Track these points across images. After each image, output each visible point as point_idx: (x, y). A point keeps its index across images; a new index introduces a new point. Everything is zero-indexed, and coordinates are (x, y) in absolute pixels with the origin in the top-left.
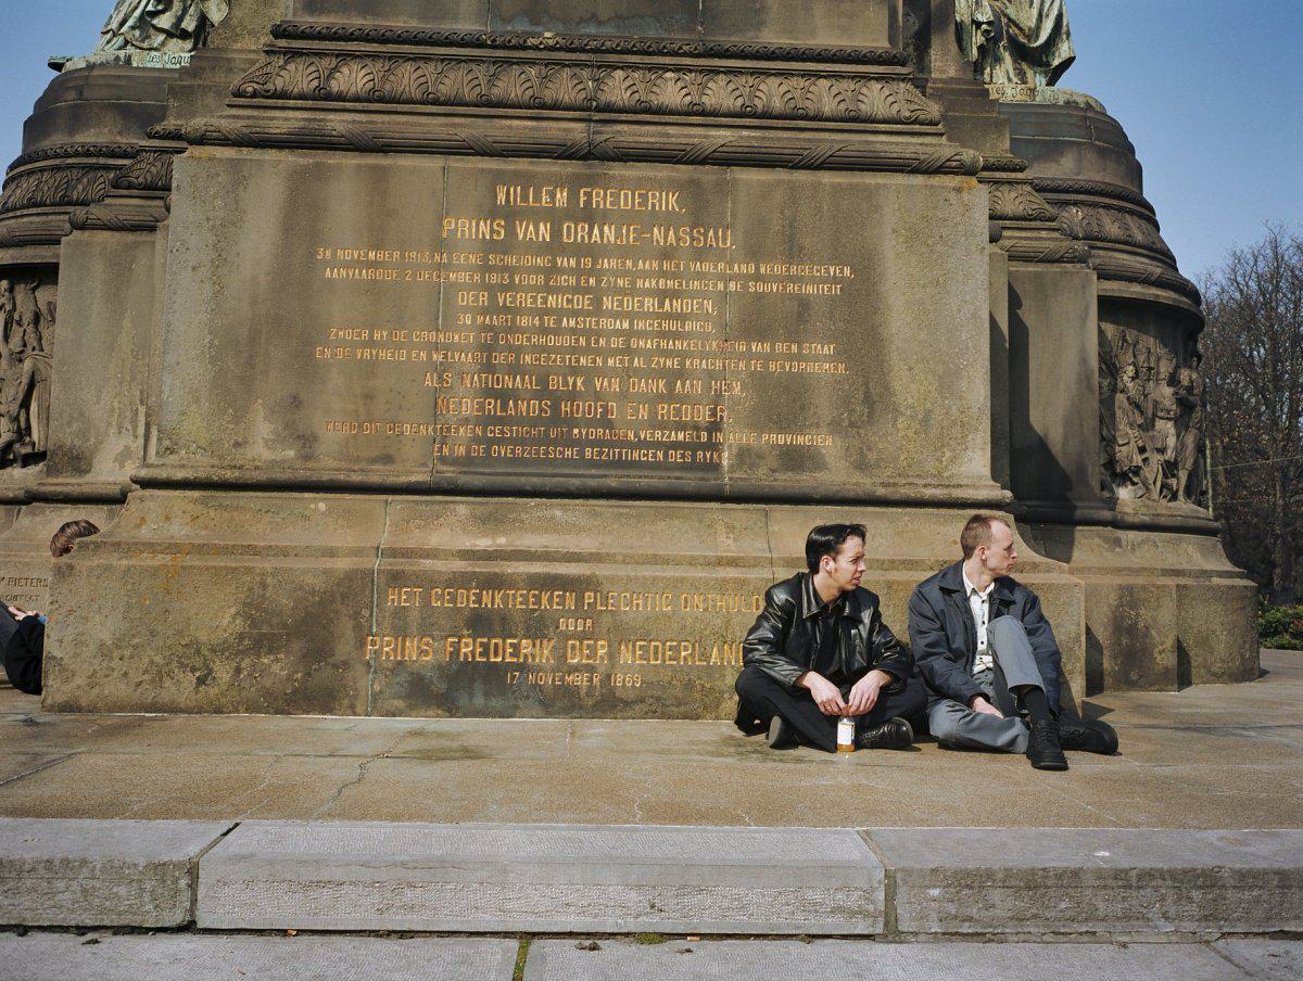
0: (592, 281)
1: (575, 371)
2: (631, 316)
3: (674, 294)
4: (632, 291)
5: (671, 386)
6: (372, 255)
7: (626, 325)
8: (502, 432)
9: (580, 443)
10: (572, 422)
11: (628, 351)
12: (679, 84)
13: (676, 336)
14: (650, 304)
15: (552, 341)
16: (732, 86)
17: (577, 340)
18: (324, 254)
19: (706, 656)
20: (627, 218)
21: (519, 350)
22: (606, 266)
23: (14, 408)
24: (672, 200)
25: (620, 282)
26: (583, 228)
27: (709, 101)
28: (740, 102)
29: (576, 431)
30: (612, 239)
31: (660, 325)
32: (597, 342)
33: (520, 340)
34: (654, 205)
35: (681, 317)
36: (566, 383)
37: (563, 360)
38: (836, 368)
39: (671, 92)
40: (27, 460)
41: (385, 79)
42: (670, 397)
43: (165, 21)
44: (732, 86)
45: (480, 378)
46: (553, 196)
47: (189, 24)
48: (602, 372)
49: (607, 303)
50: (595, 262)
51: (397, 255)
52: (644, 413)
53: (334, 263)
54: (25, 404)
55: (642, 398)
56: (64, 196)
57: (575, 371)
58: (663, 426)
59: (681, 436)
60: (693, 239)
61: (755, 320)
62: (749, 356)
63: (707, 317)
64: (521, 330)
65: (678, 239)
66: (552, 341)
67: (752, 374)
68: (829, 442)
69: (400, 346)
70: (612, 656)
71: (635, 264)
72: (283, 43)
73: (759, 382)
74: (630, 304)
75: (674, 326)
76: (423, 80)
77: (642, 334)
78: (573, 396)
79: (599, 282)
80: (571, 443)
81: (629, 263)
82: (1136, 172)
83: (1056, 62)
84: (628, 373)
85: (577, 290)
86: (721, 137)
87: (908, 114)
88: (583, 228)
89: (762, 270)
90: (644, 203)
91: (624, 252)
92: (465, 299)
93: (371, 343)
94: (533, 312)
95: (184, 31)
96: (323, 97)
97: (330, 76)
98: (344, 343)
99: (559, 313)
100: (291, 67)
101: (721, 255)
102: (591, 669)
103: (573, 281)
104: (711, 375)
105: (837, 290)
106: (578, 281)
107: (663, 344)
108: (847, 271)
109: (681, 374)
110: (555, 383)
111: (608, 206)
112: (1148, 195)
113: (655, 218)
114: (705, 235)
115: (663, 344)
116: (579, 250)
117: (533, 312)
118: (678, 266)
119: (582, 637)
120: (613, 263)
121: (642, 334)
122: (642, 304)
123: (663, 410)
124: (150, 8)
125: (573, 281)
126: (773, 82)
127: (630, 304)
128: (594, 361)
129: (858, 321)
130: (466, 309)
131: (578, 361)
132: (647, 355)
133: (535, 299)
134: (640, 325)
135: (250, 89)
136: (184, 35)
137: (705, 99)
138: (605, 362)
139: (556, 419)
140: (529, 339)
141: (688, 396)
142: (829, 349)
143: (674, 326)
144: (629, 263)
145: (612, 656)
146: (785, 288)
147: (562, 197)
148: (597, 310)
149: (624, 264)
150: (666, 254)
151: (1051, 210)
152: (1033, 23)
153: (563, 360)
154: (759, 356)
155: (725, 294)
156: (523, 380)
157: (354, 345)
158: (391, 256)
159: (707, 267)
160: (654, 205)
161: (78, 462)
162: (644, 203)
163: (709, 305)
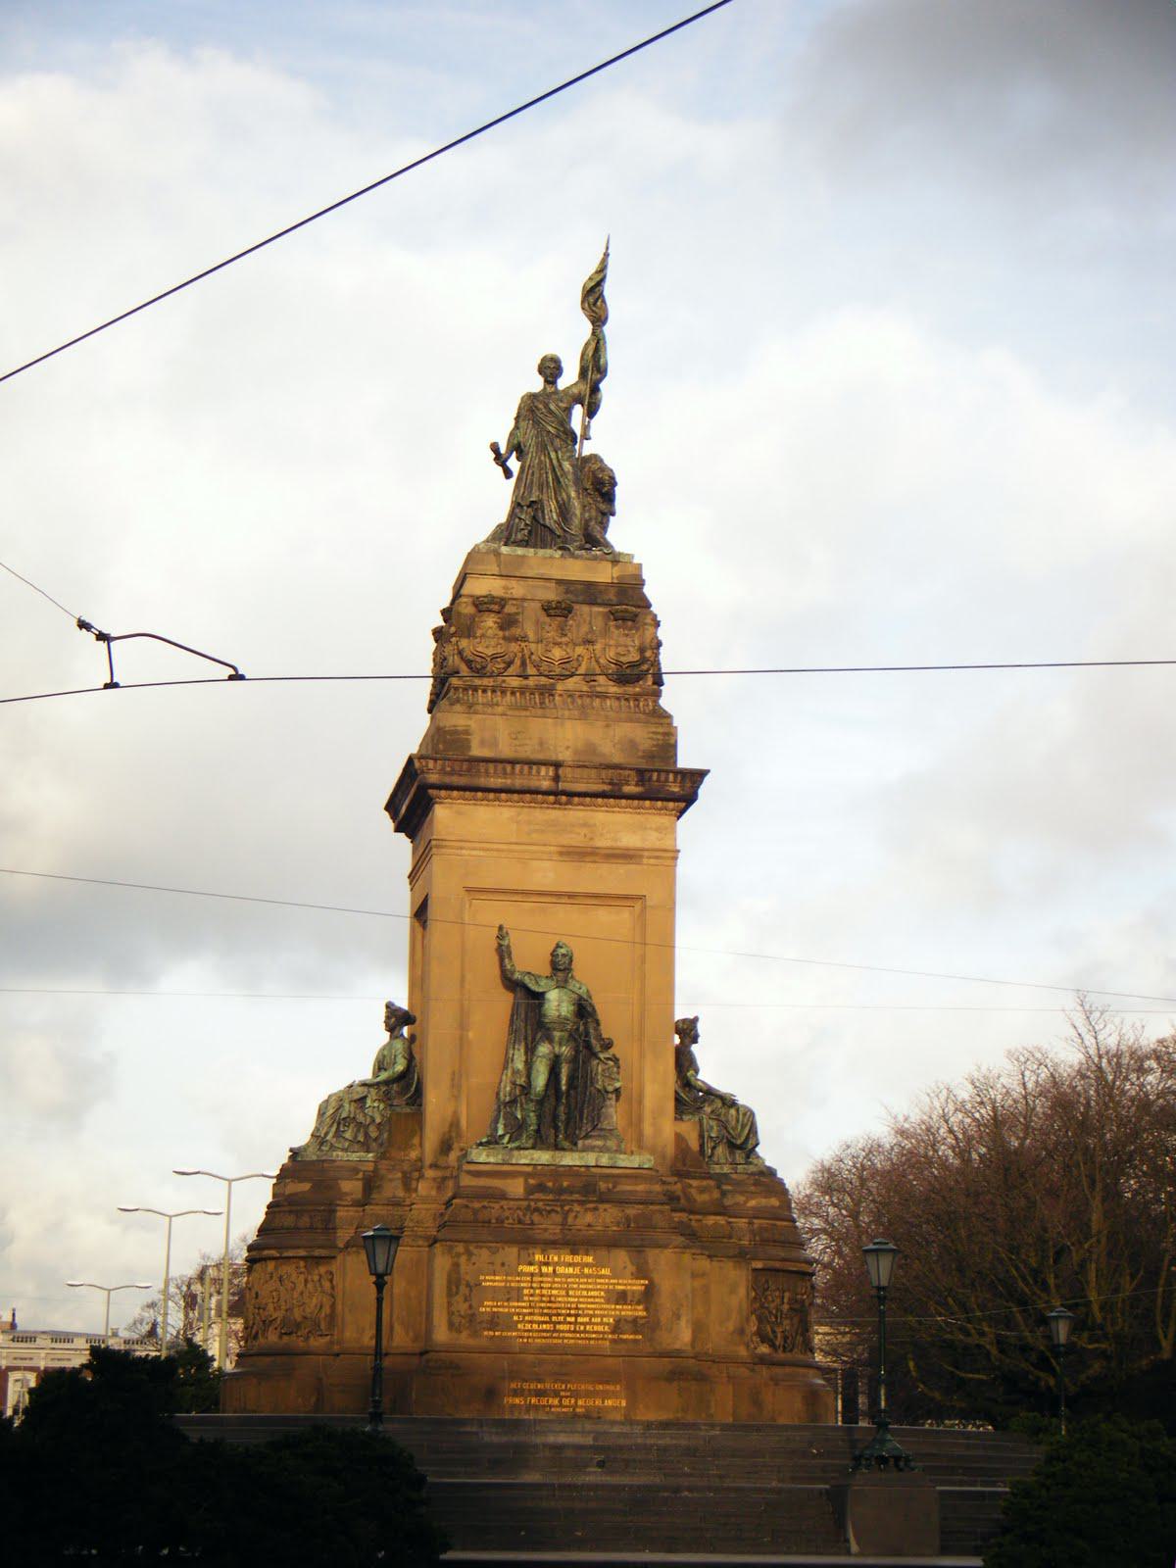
2: (578, 1297)
3: (591, 1290)
4: (579, 1289)
5: (590, 1319)
9: (564, 1338)
15: (554, 1305)
19: (603, 1403)
21: (543, 1308)
33: (543, 1305)
35: (594, 1297)
42: (590, 1323)
48: (570, 1315)
49: (571, 1293)
53: (485, 1281)
55: (581, 1324)
62: (615, 1309)
70: (576, 1402)
74: (578, 1293)
75: (592, 1300)
77: (581, 1303)
78: (559, 1323)
80: (558, 1338)
83: (750, 1147)
84: (577, 1316)
91: (577, 1276)
92: (526, 1292)
99: (556, 1296)
104: (602, 1316)
105: (643, 1288)
110: (554, 1319)
119: (567, 1397)
121: (581, 1303)
123: (588, 1328)
127: (578, 1293)
130: (526, 1295)
132: (583, 1309)
134: (581, 1300)
139: (555, 1331)
145: (576, 1402)
148: (568, 1295)
150: (588, 1276)
155: (608, 1289)
159: (602, 1281)
163: (602, 1293)
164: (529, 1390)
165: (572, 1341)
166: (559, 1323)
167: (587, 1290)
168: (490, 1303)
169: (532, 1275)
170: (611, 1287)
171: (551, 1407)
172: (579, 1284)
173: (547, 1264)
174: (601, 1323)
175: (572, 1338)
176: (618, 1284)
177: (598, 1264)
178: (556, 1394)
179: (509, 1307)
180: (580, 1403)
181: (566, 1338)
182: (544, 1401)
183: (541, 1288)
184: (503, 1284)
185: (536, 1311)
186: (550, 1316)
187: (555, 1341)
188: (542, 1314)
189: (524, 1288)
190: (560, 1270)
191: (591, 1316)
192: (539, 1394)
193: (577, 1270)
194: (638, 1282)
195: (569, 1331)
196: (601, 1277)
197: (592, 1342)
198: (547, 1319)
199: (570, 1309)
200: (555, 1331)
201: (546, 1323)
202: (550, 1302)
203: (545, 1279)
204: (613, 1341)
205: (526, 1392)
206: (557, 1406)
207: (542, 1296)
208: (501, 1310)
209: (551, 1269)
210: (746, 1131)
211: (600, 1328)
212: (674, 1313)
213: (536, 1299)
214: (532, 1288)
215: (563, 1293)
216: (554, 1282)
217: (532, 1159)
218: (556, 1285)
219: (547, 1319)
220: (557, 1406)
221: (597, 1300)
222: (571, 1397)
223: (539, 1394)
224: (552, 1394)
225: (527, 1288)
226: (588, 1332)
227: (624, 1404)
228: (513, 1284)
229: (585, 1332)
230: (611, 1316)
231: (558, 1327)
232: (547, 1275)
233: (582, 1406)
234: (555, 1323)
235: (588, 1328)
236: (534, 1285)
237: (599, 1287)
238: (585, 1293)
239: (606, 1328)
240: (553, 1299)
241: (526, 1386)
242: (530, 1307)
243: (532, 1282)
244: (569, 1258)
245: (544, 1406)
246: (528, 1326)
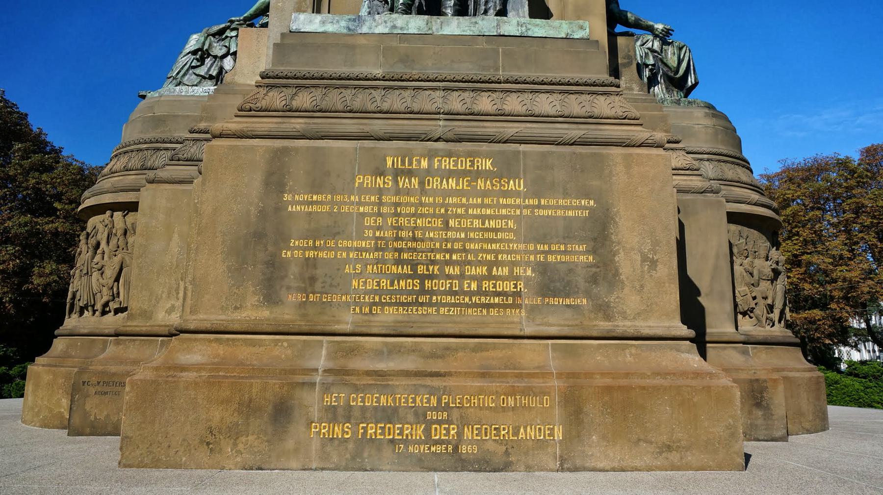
0: (443, 211)
1: (433, 262)
2: (466, 230)
3: (490, 217)
4: (466, 216)
5: (490, 270)
6: (315, 198)
7: (463, 236)
8: (390, 298)
9: (439, 305)
10: (432, 293)
11: (465, 250)
12: (490, 99)
13: (492, 241)
14: (477, 223)
16: (520, 99)
17: (434, 245)
18: (287, 197)
20: (463, 174)
21: (400, 251)
22: (451, 201)
23: (111, 281)
24: (489, 163)
25: (459, 211)
26: (437, 181)
27: (508, 108)
28: (525, 108)
29: (434, 298)
30: (454, 185)
31: (483, 235)
32: (446, 245)
34: (478, 167)
35: (496, 230)
36: (428, 270)
37: (427, 256)
38: (587, 259)
39: (485, 103)
40: (117, 311)
41: (322, 99)
42: (490, 277)
43: (202, 71)
44: (520, 99)
45: (377, 268)
46: (419, 162)
47: (214, 72)
48: (449, 263)
49: (452, 223)
50: (444, 200)
51: (329, 197)
52: (474, 286)
54: (117, 280)
55: (473, 278)
56: (143, 165)
57: (433, 262)
58: (486, 294)
59: (496, 300)
60: (501, 185)
61: (538, 232)
62: (536, 252)
63: (510, 230)
64: (402, 239)
65: (493, 185)
66: (420, 246)
67: (539, 264)
68: (585, 301)
69: (330, 249)
70: (460, 434)
71: (468, 200)
72: (267, 81)
73: (543, 269)
75: (491, 235)
76: (344, 99)
77: (471, 240)
79: (446, 211)
80: (430, 304)
81: (464, 200)
82: (738, 143)
85: (434, 216)
86: (511, 129)
87: (621, 114)
88: (437, 181)
89: (542, 203)
90: (472, 165)
92: (369, 222)
93: (315, 248)
94: (408, 229)
95: (211, 75)
96: (289, 111)
97: (292, 99)
98: (298, 248)
99: (424, 229)
100: (271, 94)
101: (517, 194)
102: (448, 442)
103: (431, 211)
104: (513, 264)
106: (435, 211)
107: (485, 246)
108: (592, 202)
109: (497, 263)
110: (421, 269)
111: (452, 168)
112: (746, 154)
113: (478, 174)
114: (508, 183)
115: (485, 246)
116: (434, 193)
117: (408, 229)
118: (493, 201)
119: (440, 422)
120: (455, 199)
121: (471, 240)
122: (472, 223)
123: (485, 285)
124: (193, 64)
125: (431, 211)
126: (543, 96)
128: (444, 257)
129: (599, 232)
131: (435, 256)
132: (476, 252)
133: (409, 221)
135: (248, 107)
136: (211, 77)
137: (505, 107)
138: (451, 256)
139: (423, 291)
140: (406, 244)
141: (500, 276)
142: (583, 248)
143: (491, 235)
144: (464, 200)
145: (460, 434)
146: (556, 212)
147: (424, 164)
148: (447, 227)
149: (461, 200)
150: (485, 194)
151: (696, 163)
152: (675, 65)
153: (427, 256)
154: (543, 252)
156: (403, 268)
157: (305, 249)
158: (326, 198)
159: (510, 201)
160: (478, 167)
161: (146, 315)
162: (472, 165)
163: (511, 224)
164: (363, 409)
165: (454, 311)
166: (431, 277)
167: (483, 218)
168: (302, 243)
169: (380, 192)
170: (526, 212)
171: (406, 442)
172: (467, 207)
173: (410, 173)
174: (512, 277)
175: (455, 305)
176: (539, 207)
177: (507, 169)
178: (420, 415)
179: (336, 249)
180: (467, 433)
181: (444, 305)
182: (394, 431)
183: (397, 215)
184: (326, 208)
185: (389, 256)
186: (414, 265)
187: (422, 311)
188: (399, 262)
189: (363, 215)
190: (435, 183)
191: (490, 265)
192: (389, 415)
193: (464, 184)
194: (576, 202)
195: (451, 293)
196: (506, 194)
197: (493, 312)
198: (407, 270)
199: (451, 251)
200: (423, 291)
201: (407, 277)
202: (414, 239)
203: (404, 199)
204: (533, 310)
205: (357, 413)
206: (419, 442)
207: (400, 228)
208: (322, 255)
209: (415, 181)
210: (684, 65)
211: (509, 286)
212: (644, 259)
213: (388, 234)
214: (379, 214)
215: (439, 223)
216: (421, 204)
217: (394, 27)
218: (425, 210)
219: (407, 270)
220: (419, 442)
221: (500, 235)
222: (449, 422)
223: (389, 415)
224: (411, 417)
225: (370, 215)
226: (486, 294)
227: (559, 434)
228: (345, 209)
229: (479, 292)
230: (528, 264)
231: (428, 284)
232: (408, 192)
233: (471, 442)
234: (423, 278)
235: (485, 285)
236: (385, 210)
237: (504, 212)
238: (477, 223)
239: (521, 285)
240: (419, 234)
241: (356, 401)
242: (377, 249)
243: (380, 204)
244: (448, 164)
245: (392, 441)
246: (372, 285)
